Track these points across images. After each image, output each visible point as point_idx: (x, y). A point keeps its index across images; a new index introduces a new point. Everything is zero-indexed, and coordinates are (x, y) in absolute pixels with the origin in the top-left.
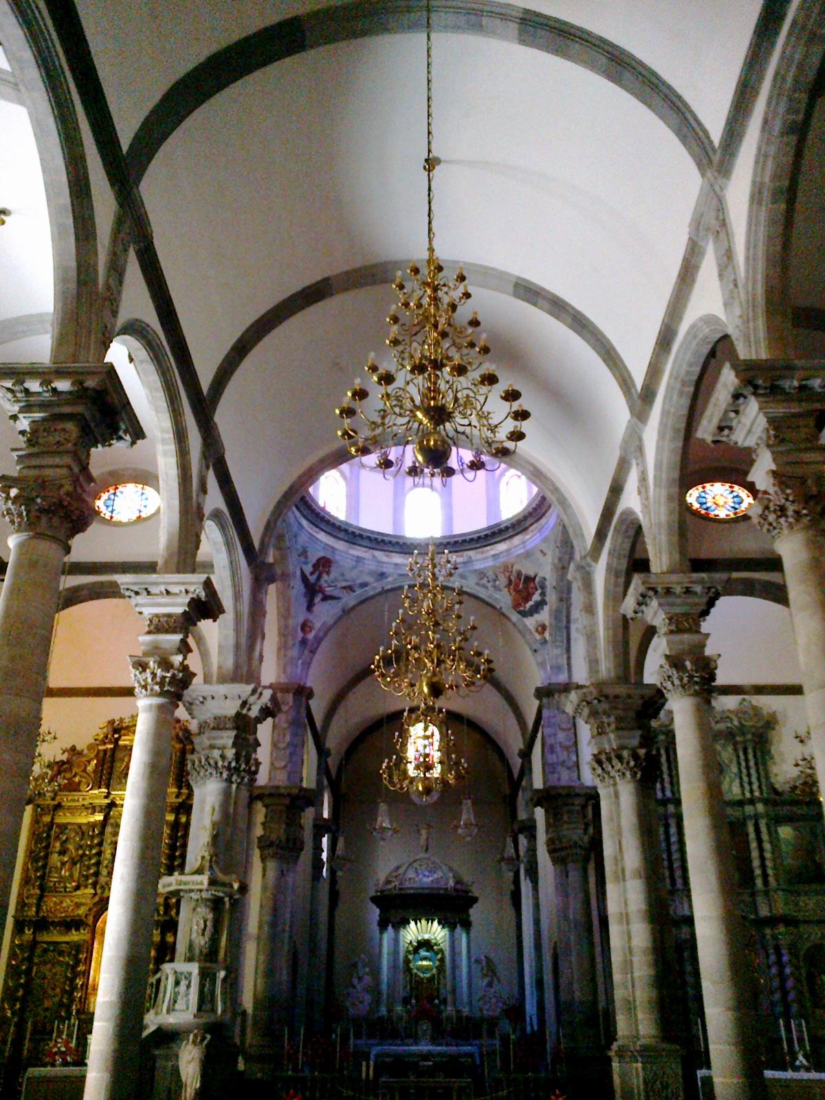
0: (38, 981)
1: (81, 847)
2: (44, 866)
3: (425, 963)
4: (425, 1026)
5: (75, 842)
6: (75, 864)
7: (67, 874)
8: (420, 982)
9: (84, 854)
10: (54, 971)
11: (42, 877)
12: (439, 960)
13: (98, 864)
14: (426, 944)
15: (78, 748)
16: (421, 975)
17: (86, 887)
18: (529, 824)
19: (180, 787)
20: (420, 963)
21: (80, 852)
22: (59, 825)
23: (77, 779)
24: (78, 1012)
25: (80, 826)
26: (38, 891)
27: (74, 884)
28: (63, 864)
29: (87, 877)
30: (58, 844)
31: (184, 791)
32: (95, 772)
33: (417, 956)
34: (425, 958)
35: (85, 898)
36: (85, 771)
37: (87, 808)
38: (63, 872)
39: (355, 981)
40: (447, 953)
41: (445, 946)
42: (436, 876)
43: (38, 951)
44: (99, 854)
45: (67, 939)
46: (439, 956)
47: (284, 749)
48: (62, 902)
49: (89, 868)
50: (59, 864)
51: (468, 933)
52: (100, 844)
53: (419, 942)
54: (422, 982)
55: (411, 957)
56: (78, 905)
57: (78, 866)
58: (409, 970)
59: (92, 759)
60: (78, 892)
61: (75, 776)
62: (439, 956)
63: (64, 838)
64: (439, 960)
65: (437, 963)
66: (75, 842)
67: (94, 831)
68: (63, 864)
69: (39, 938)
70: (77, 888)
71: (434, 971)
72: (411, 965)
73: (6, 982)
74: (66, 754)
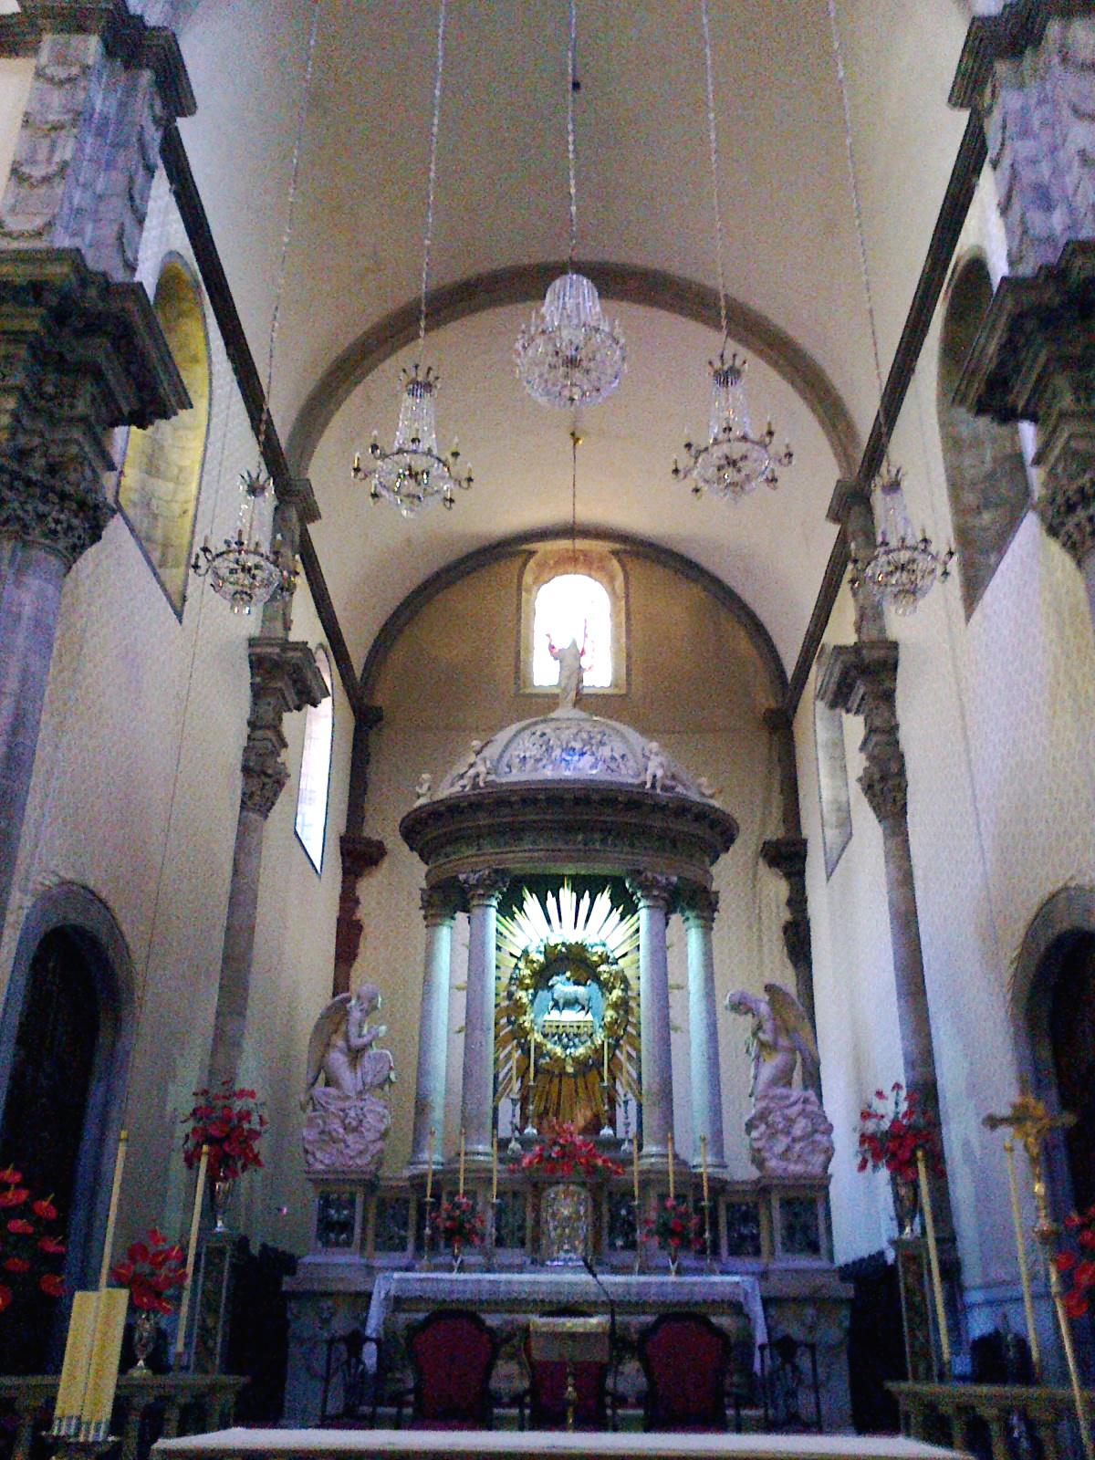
3: (570, 1016)
4: (566, 1204)
8: (551, 1073)
12: (615, 1006)
14: (573, 961)
16: (558, 1050)
18: (878, 654)
20: (555, 1015)
33: (543, 994)
34: (571, 1003)
39: (338, 1059)
40: (643, 986)
41: (638, 969)
42: (605, 752)
46: (617, 993)
47: (46, 179)
51: (707, 929)
53: (548, 951)
54: (563, 1074)
55: (524, 996)
58: (520, 1034)
62: (617, 993)
64: (615, 1006)
65: (610, 1014)
71: (600, 1037)
72: (526, 1020)
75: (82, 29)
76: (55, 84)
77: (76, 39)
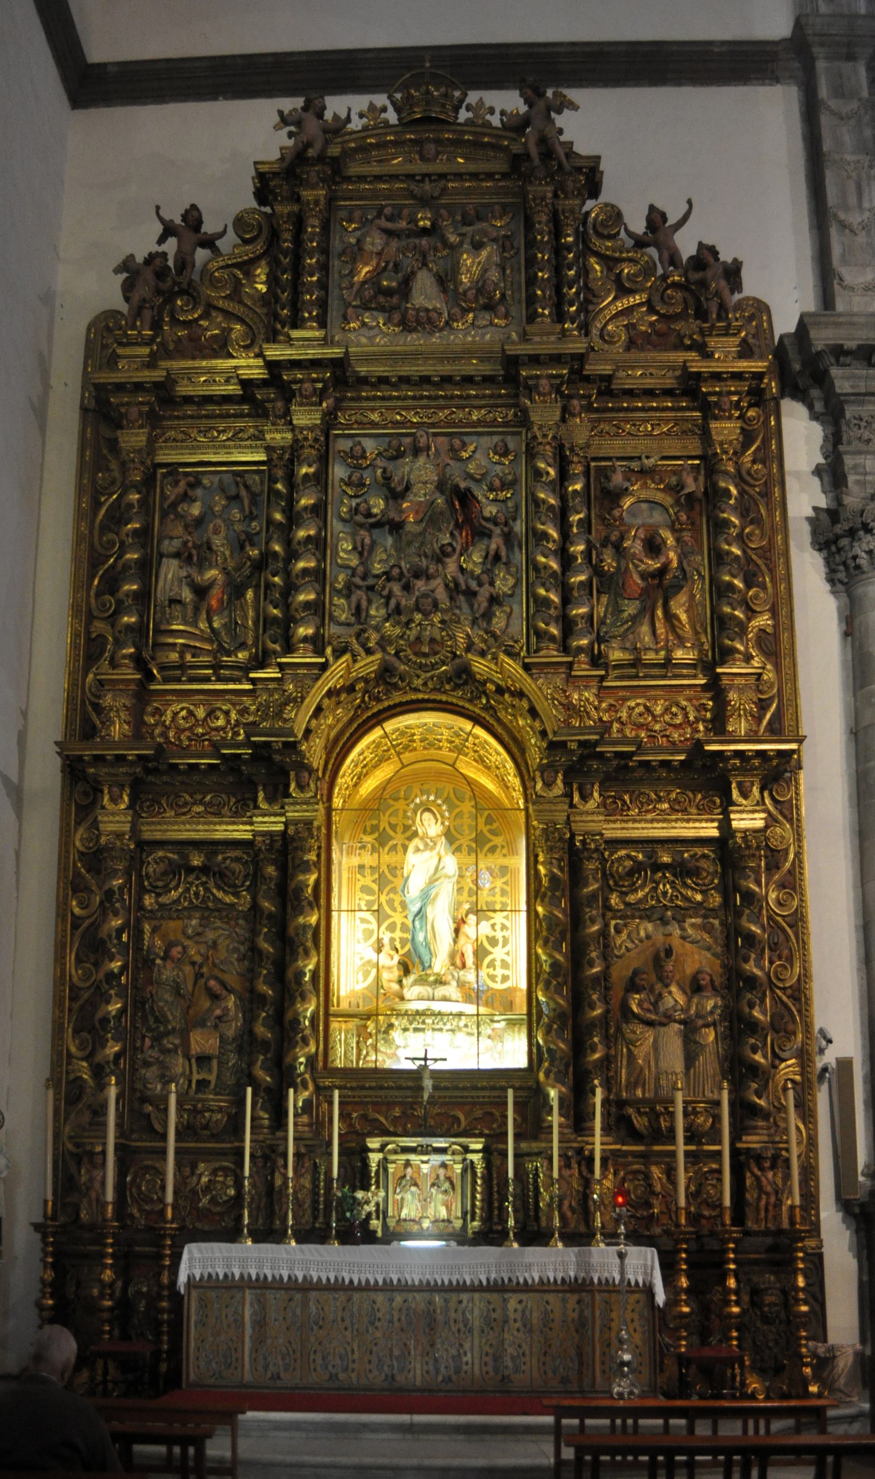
1: (250, 539)
5: (229, 523)
6: (236, 591)
9: (268, 556)
10: (211, 935)
15: (209, 227)
24: (311, 1061)
28: (201, 592)
45: (240, 831)
50: (187, 595)
57: (250, 594)
59: (253, 262)
63: (196, 510)
66: (229, 523)
75: (851, 57)
76: (842, 119)
77: (846, 67)
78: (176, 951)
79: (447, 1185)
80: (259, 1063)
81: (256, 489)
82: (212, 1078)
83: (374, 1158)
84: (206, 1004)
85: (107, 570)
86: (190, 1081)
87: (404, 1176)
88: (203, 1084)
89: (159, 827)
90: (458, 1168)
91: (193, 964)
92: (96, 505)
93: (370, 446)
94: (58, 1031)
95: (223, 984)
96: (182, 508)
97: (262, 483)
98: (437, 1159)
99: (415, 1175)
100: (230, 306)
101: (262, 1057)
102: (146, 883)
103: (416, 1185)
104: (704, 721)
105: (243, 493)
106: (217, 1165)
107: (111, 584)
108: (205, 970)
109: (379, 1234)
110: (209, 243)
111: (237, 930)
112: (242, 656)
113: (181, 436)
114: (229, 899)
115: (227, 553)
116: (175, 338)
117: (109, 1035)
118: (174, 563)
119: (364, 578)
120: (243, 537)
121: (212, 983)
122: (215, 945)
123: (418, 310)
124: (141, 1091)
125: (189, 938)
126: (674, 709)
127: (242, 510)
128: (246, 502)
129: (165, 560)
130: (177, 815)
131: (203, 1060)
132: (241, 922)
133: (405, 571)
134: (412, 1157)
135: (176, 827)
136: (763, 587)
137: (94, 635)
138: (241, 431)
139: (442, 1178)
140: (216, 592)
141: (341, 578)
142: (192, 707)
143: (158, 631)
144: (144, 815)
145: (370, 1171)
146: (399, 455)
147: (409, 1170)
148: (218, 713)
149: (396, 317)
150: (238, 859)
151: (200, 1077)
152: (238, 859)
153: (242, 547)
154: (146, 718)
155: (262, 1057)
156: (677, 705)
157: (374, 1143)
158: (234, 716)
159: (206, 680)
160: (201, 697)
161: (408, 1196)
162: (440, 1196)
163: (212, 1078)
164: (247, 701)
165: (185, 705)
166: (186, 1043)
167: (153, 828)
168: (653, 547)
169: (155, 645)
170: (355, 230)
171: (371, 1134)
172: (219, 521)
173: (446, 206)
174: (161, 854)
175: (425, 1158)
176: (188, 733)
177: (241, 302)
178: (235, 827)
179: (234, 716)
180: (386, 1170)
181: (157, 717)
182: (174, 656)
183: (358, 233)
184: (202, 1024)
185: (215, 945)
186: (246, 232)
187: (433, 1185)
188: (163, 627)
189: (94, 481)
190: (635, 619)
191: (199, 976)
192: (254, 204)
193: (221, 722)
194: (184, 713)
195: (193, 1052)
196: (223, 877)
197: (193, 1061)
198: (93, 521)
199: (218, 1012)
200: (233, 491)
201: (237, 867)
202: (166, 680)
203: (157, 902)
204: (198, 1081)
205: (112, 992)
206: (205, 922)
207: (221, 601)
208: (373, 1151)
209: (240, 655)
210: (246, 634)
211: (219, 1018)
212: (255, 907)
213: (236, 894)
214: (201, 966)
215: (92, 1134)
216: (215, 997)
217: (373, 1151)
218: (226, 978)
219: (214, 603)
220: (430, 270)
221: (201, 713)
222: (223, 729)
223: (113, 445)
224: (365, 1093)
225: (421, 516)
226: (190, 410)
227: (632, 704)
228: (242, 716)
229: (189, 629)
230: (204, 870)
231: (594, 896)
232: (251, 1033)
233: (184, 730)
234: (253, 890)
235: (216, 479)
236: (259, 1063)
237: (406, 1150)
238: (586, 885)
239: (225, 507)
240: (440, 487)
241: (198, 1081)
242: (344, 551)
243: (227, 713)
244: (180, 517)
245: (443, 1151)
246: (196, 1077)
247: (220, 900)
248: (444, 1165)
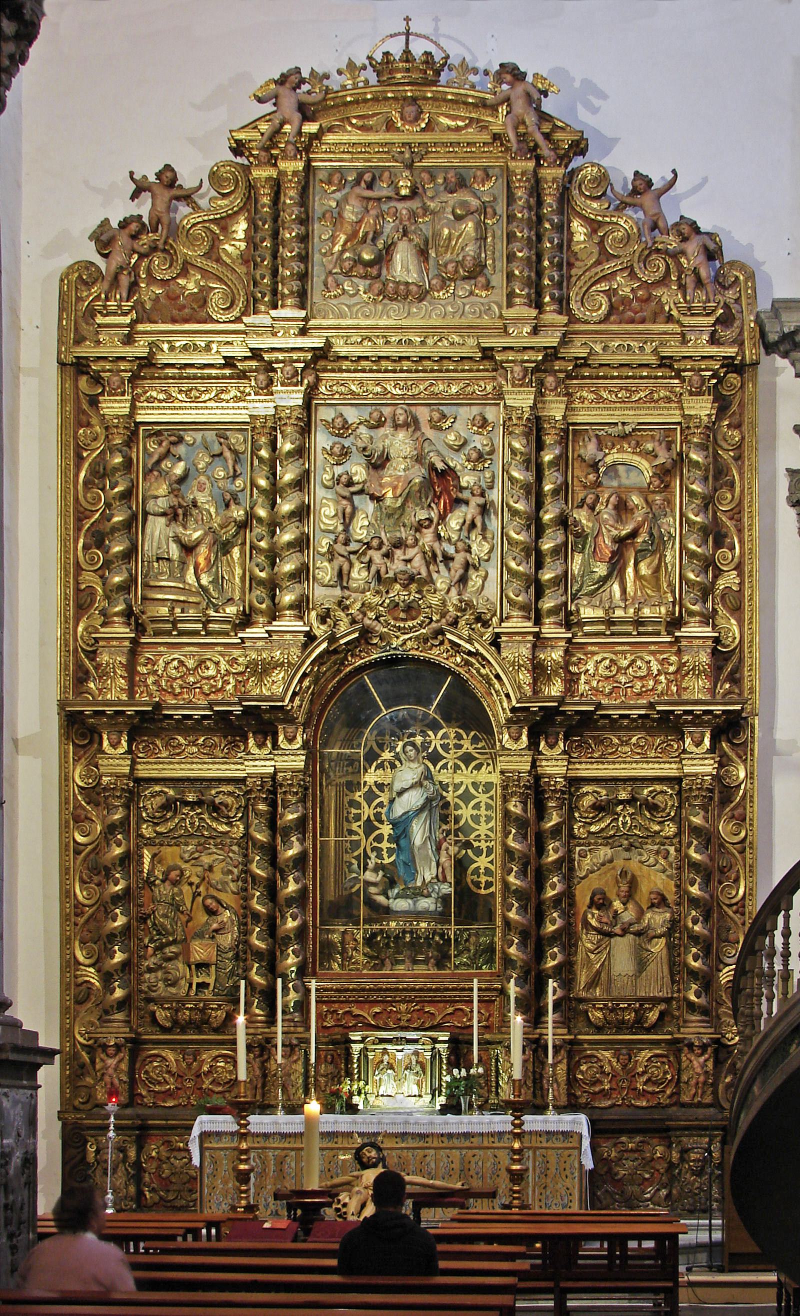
0: (165, 890)
2: (130, 554)
5: (213, 480)
6: (225, 548)
7: (205, 580)
10: (206, 860)
11: (126, 587)
13: (302, 544)
15: (187, 180)
17: (274, 614)
19: (539, 306)
21: (238, 513)
22: (156, 432)
23: (190, 285)
25: (222, 430)
26: (121, 630)
27: (231, 610)
28: (188, 549)
29: (272, 586)
30: (163, 489)
31: (551, 316)
32: (246, 259)
35: (283, 646)
36: (213, 253)
37: (243, 375)
38: (190, 578)
43: (151, 804)
44: (302, 513)
48: (201, 663)
49: (273, 556)
50: (174, 551)
52: (302, 483)
56: (262, 670)
57: (236, 552)
59: (232, 217)
60: (250, 632)
61: (184, 272)
63: (179, 469)
67: (273, 445)
68: (188, 549)
69: (143, 771)
70: (246, 620)
73: (66, 894)
74: (146, 197)
78: (174, 874)
79: (418, 1068)
80: (255, 970)
81: (241, 448)
82: (211, 980)
83: (356, 1048)
84: (203, 918)
85: (92, 524)
86: (191, 985)
87: (382, 1061)
88: (202, 986)
89: (155, 766)
90: (428, 1055)
91: (191, 884)
92: (80, 459)
93: (352, 415)
94: (66, 942)
95: (219, 902)
96: (166, 464)
97: (245, 441)
98: (412, 1047)
99: (392, 1061)
100: (212, 266)
101: (256, 965)
102: (144, 815)
103: (392, 1068)
104: (666, 673)
105: (227, 454)
106: (216, 1053)
107: (98, 539)
108: (201, 889)
109: (361, 1107)
110: (187, 198)
111: (231, 855)
112: (231, 610)
113: (161, 396)
114: (223, 828)
115: (213, 510)
116: (154, 296)
117: (116, 948)
118: (162, 520)
119: (346, 543)
120: (228, 497)
121: (209, 901)
122: (211, 868)
123: (398, 283)
124: (146, 993)
125: (186, 862)
126: (639, 663)
127: (226, 468)
128: (230, 463)
129: (150, 517)
130: (171, 756)
131: (202, 966)
132: (235, 848)
133: (385, 541)
134: (389, 1046)
135: (171, 766)
136: (732, 548)
137: (83, 587)
138: (222, 392)
139: (414, 1063)
140: (203, 550)
141: (324, 542)
142: (182, 658)
143: (146, 585)
144: (140, 755)
145: (353, 1058)
146: (380, 424)
147: (386, 1057)
148: (208, 663)
149: (378, 286)
150: (230, 794)
151: (200, 980)
152: (230, 794)
153: (227, 506)
154: (139, 668)
155: (256, 965)
156: (642, 659)
157: (355, 1036)
158: (223, 666)
159: (196, 633)
160: (191, 649)
161: (385, 1077)
162: (412, 1077)
163: (211, 980)
164: (236, 653)
165: (176, 656)
166: (186, 952)
167: (150, 766)
168: (622, 508)
169: (144, 598)
170: (334, 192)
171: (354, 1028)
172: (203, 479)
173: (426, 169)
174: (158, 788)
175: (400, 1047)
176: (179, 682)
177: (218, 260)
178: (227, 767)
179: (223, 666)
180: (366, 1057)
181: (149, 666)
182: (164, 611)
183: (338, 195)
184: (200, 935)
185: (211, 868)
186: (225, 187)
187: (406, 1068)
188: (152, 583)
189: (76, 437)
190: (604, 580)
191: (196, 895)
192: (230, 156)
193: (212, 672)
194: (175, 663)
195: (192, 960)
196: (215, 809)
197: (193, 967)
198: (77, 476)
199: (215, 926)
200: (216, 449)
201: (229, 800)
202: (157, 633)
203: (155, 832)
204: (198, 985)
205: (118, 911)
206: (202, 847)
207: (208, 559)
208: (355, 1042)
209: (228, 610)
210: (233, 590)
211: (216, 931)
212: (247, 835)
213: (229, 824)
214: (198, 887)
215: (104, 1030)
216: (211, 912)
217: (355, 1042)
218: (222, 896)
219: (201, 560)
220: (410, 240)
221: (191, 663)
222: (213, 677)
223: (94, 402)
224: (349, 994)
225: (398, 492)
226: (170, 371)
227: (598, 658)
228: (232, 666)
229: (181, 586)
230: (199, 803)
231: (556, 831)
232: (246, 942)
233: (176, 679)
234: (245, 819)
235: (199, 436)
236: (255, 970)
237: (382, 1041)
238: (551, 820)
239: (209, 464)
240: (419, 459)
241: (198, 985)
242: (326, 516)
243: (217, 664)
244: (166, 474)
245: (415, 1041)
246: (196, 980)
247: (215, 829)
248: (416, 1053)
